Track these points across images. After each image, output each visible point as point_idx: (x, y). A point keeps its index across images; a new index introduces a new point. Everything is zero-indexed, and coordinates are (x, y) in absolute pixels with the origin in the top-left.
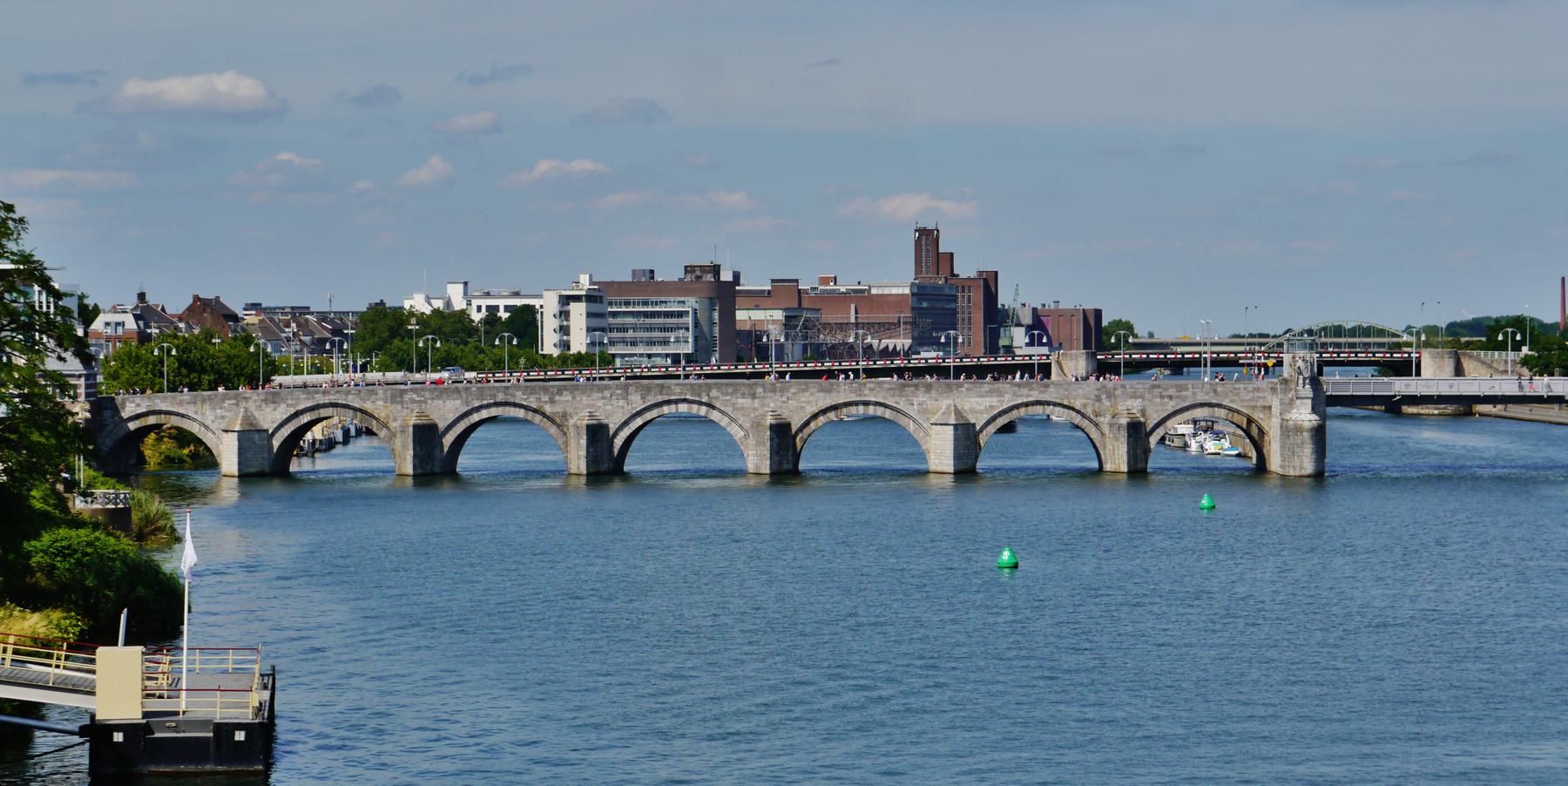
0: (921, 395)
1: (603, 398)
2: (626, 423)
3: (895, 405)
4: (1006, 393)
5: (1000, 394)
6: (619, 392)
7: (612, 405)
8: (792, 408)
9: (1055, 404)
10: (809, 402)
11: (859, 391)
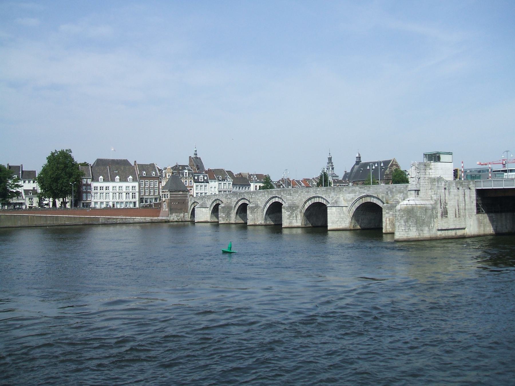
0: (332, 193)
1: (261, 196)
2: (265, 206)
3: (325, 198)
4: (357, 191)
5: (355, 193)
6: (263, 194)
7: (262, 199)
8: (300, 200)
9: (374, 197)
10: (303, 197)
11: (315, 192)
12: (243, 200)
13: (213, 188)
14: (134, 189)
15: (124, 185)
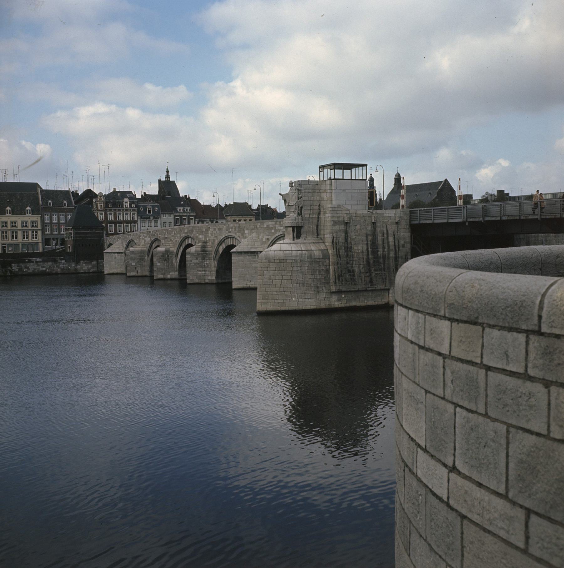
12: (156, 241)
13: (167, 224)
14: (35, 226)
15: (19, 219)
